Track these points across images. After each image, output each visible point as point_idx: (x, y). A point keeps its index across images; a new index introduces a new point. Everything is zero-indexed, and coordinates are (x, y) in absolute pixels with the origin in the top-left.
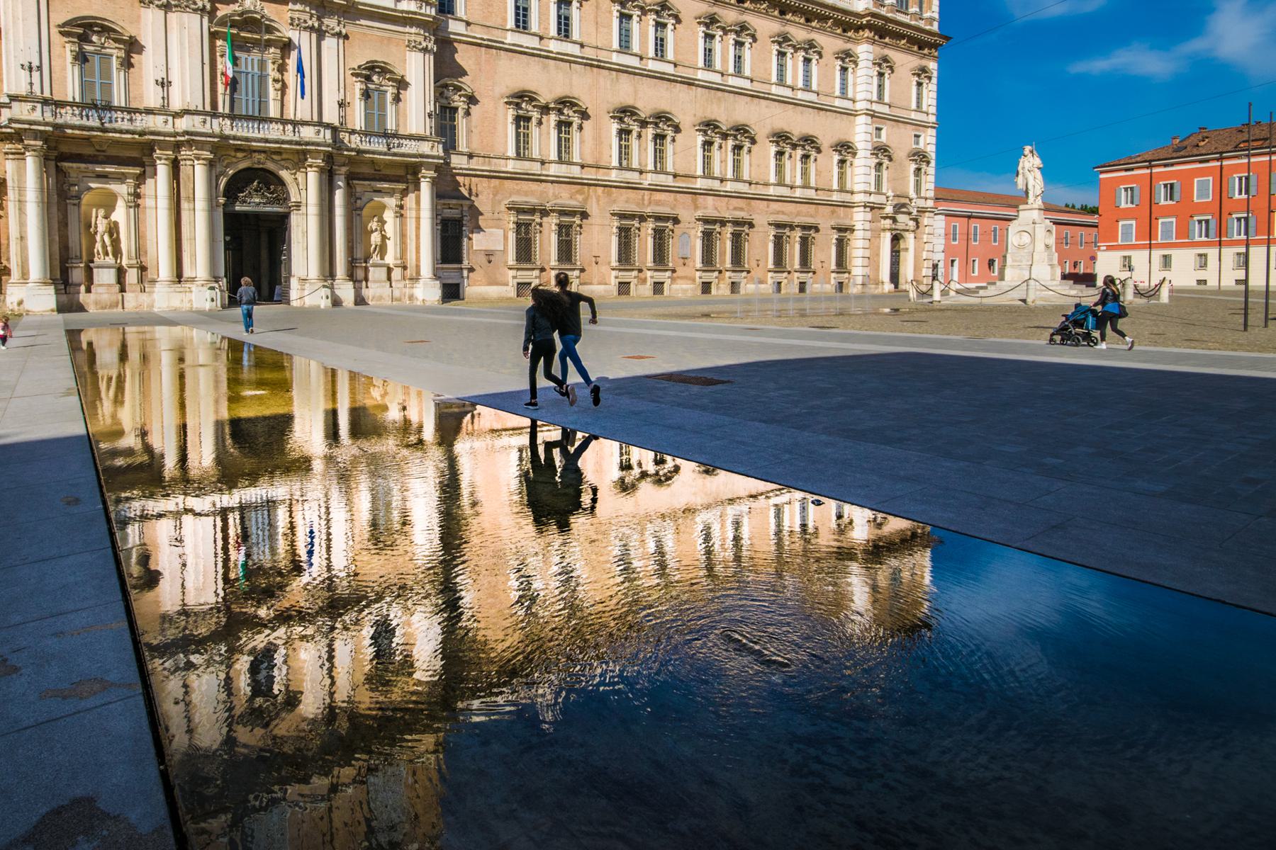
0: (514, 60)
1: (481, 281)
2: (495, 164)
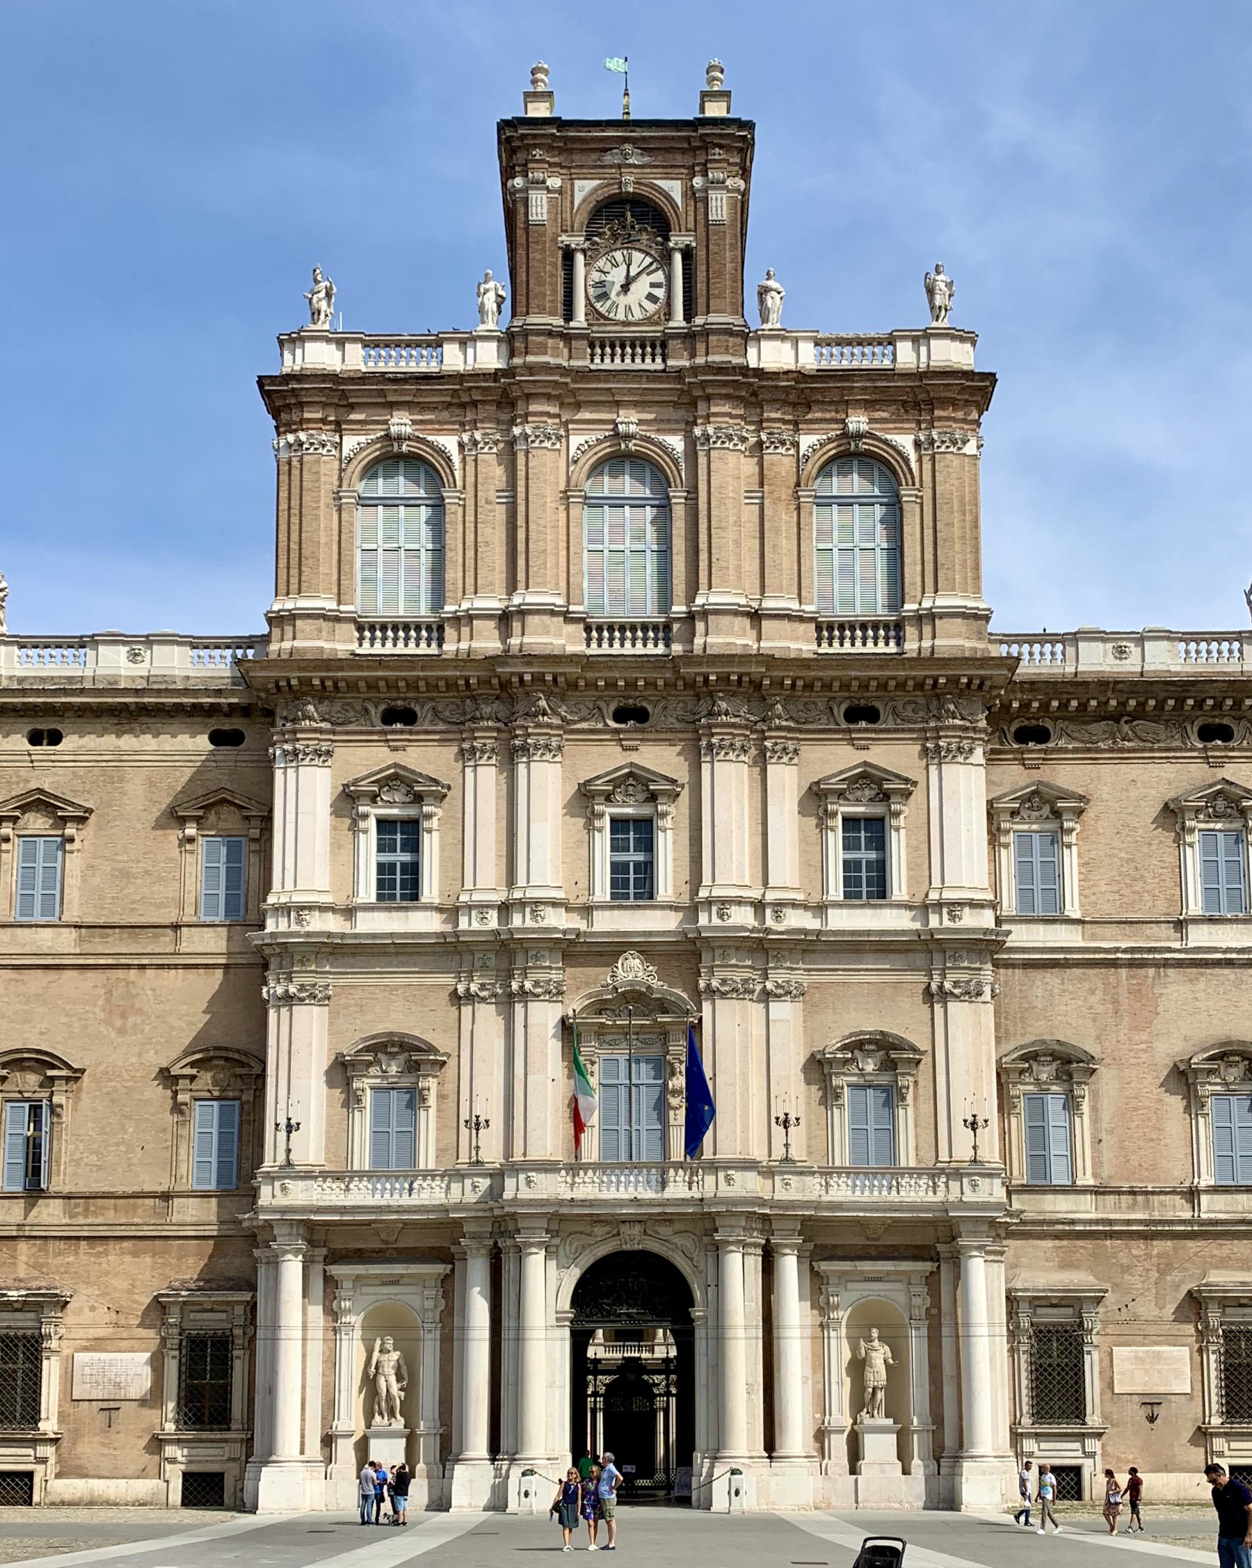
0: (1202, 985)
2: (1162, 1204)
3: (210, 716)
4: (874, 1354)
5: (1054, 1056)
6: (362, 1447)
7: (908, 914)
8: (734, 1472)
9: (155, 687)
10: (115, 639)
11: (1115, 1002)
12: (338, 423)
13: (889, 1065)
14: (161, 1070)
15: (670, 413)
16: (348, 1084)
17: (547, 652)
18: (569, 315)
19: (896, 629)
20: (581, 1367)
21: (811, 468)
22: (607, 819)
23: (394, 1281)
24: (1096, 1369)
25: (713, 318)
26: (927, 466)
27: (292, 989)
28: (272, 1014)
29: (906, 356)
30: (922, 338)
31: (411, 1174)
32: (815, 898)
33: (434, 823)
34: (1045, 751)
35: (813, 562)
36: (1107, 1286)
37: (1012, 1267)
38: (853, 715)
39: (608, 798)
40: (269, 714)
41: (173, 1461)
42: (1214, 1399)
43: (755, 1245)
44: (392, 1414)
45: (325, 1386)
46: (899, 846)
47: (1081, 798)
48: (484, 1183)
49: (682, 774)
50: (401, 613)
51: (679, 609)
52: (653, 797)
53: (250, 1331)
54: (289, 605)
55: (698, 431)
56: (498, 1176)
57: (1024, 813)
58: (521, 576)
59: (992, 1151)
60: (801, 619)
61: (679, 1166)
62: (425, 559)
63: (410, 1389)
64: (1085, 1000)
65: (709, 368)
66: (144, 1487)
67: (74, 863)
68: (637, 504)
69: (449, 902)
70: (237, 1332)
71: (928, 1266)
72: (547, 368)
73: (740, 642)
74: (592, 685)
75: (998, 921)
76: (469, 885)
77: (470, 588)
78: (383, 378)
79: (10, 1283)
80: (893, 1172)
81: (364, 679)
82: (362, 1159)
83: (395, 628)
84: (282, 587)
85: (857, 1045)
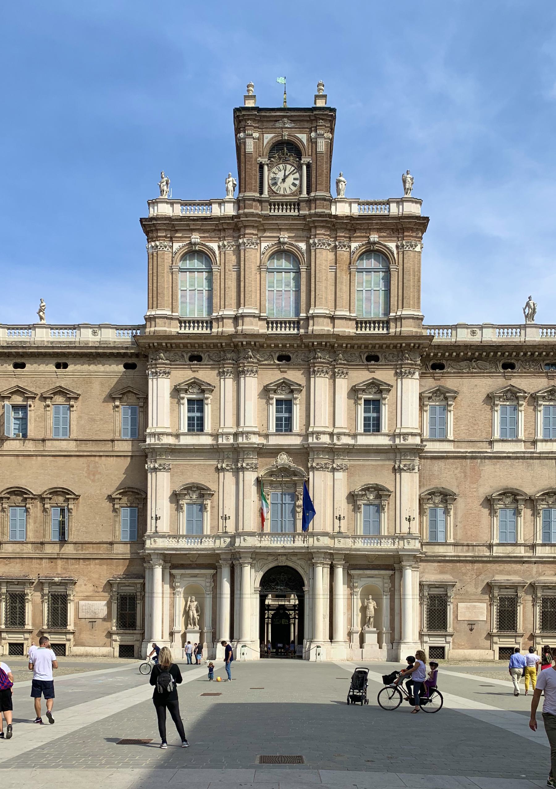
0: (498, 466)
1: (464, 645)
2: (479, 550)
3: (124, 357)
4: (370, 605)
5: (441, 493)
6: (184, 636)
7: (388, 438)
8: (318, 647)
9: (103, 345)
10: (86, 326)
11: (465, 472)
12: (171, 238)
13: (379, 497)
14: (109, 496)
15: (300, 233)
16: (178, 502)
17: (252, 333)
18: (261, 193)
19: (387, 324)
20: (263, 608)
21: (355, 256)
22: (275, 400)
23: (195, 576)
24: (452, 611)
25: (318, 193)
26: (401, 256)
27: (157, 466)
28: (149, 475)
29: (394, 210)
30: (400, 202)
31: (201, 536)
32: (353, 432)
33: (209, 401)
34: (443, 373)
35: (355, 296)
36: (457, 580)
37: (421, 573)
38: (369, 359)
39: (275, 392)
40: (146, 356)
41: (116, 641)
42: (495, 623)
43: (327, 564)
44: (195, 624)
45: (170, 614)
46: (385, 411)
47: (455, 392)
48: (228, 540)
49: (303, 382)
50: (196, 316)
51: (303, 315)
52: (292, 391)
53: (143, 594)
54: (153, 313)
55: (311, 241)
56: (233, 537)
57: (433, 398)
58: (242, 301)
59: (416, 529)
60: (350, 319)
61: (299, 534)
62: (205, 294)
63: (201, 615)
64: (454, 472)
65: (316, 215)
66: (105, 650)
67: (74, 415)
68: (287, 271)
69: (215, 432)
70: (138, 594)
71: (391, 572)
72: (253, 215)
73: (326, 328)
74: (269, 346)
75: (422, 441)
76: (222, 426)
77: (222, 306)
78: (188, 219)
79: (55, 575)
80: (379, 537)
81: (183, 343)
82: (183, 531)
83: (194, 322)
84: (150, 306)
85: (367, 489)
